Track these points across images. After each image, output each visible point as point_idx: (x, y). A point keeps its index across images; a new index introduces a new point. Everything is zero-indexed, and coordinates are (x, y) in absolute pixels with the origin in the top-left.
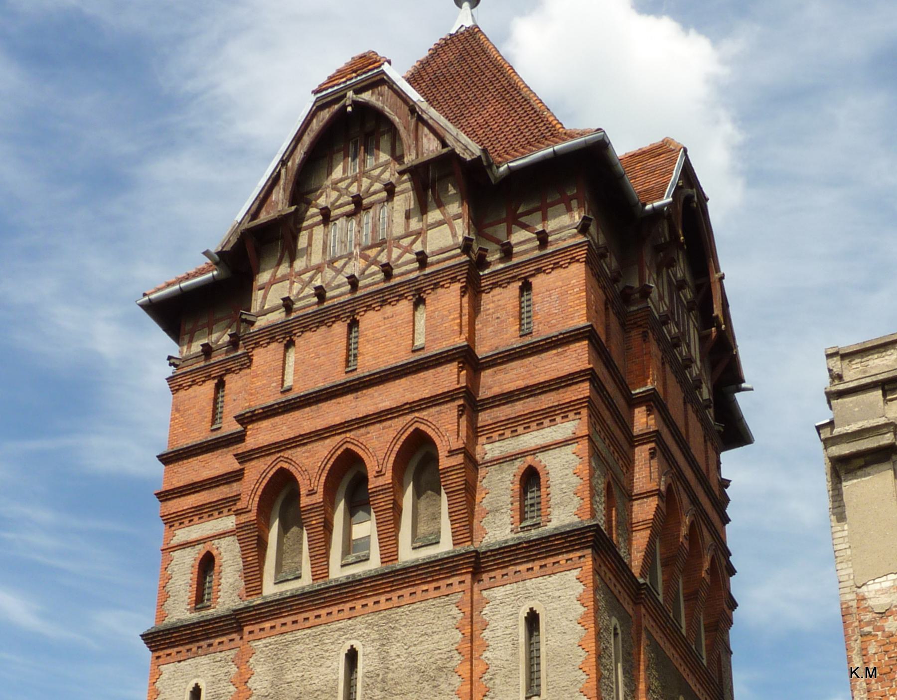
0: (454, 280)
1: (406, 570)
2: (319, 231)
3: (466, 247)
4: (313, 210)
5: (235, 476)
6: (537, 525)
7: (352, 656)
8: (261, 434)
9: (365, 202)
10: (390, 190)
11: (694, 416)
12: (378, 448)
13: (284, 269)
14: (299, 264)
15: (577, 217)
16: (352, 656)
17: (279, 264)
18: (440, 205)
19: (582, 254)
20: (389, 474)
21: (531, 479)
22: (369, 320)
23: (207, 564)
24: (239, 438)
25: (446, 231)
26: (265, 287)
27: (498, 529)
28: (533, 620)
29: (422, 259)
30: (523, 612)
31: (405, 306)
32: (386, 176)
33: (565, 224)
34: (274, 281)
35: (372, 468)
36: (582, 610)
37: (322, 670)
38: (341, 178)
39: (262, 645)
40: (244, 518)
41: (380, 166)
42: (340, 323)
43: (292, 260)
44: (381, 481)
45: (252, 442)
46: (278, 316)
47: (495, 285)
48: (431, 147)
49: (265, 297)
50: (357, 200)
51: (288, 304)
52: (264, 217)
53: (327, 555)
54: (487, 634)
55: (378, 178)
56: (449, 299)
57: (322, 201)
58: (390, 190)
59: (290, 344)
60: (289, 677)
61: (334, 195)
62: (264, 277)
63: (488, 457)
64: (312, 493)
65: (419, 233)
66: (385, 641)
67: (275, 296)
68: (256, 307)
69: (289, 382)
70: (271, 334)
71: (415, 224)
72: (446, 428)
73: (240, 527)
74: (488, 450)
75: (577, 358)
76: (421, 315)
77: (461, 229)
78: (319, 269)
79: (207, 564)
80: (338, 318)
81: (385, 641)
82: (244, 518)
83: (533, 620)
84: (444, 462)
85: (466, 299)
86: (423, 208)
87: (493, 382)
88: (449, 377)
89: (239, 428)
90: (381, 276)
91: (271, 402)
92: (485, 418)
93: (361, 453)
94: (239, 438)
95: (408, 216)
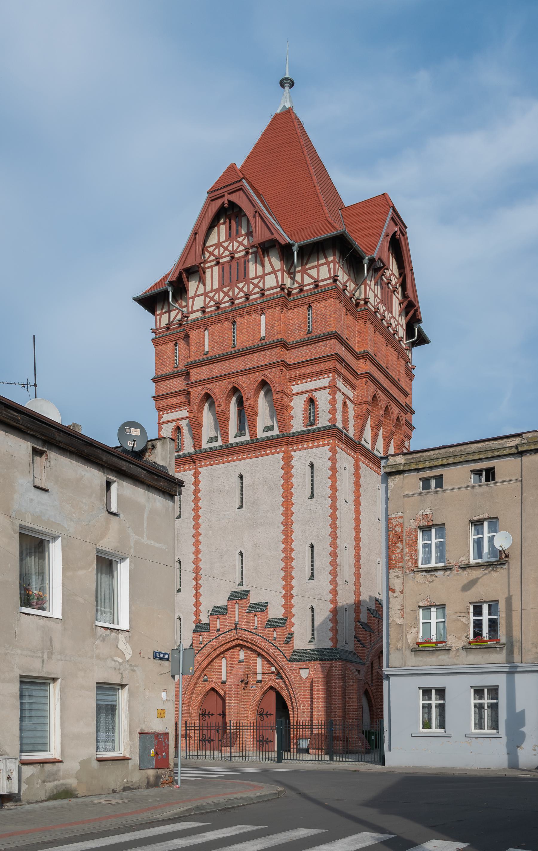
11: (382, 441)
42: (228, 322)
46: (199, 314)
93: (240, 388)
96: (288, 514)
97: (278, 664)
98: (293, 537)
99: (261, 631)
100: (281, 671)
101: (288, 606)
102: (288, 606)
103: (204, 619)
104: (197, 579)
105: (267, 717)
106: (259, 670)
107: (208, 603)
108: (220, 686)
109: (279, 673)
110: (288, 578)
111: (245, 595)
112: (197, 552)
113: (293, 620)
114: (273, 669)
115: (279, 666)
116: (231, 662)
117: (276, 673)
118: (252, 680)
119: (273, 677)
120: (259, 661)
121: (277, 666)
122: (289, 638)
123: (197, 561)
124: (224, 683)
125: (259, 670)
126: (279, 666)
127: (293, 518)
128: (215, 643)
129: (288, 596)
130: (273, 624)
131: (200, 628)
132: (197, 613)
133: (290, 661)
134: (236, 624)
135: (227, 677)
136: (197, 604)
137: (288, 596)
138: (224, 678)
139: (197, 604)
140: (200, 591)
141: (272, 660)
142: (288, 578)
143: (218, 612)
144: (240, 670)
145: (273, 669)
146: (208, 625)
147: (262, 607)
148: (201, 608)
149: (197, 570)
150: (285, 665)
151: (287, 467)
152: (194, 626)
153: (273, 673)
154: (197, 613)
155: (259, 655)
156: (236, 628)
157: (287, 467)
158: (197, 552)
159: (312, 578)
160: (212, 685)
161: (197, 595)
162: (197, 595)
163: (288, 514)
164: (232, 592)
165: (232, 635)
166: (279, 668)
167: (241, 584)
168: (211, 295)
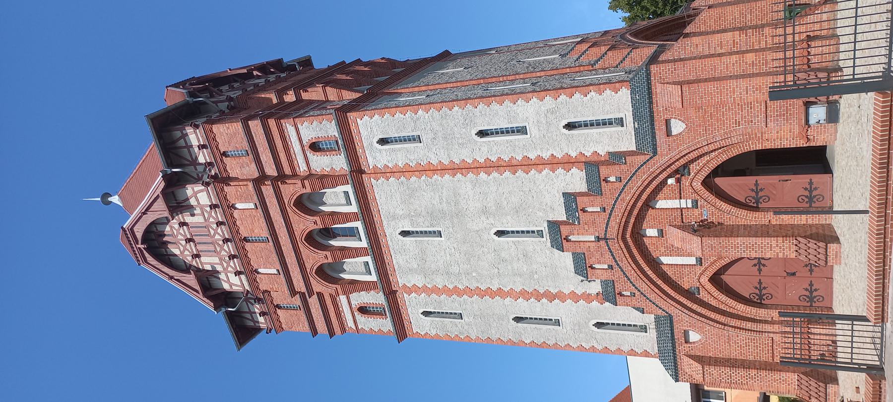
0: (222, 190)
1: (360, 207)
2: (203, 259)
3: (207, 184)
4: (194, 263)
5: (320, 296)
6: (337, 142)
7: (405, 234)
8: (300, 285)
9: (189, 237)
10: (183, 224)
12: (304, 224)
13: (222, 276)
14: (219, 268)
15: (189, 130)
16: (405, 234)
17: (219, 278)
18: (188, 199)
19: (207, 126)
20: (315, 218)
21: (315, 147)
22: (244, 233)
23: (363, 310)
24: (302, 295)
25: (199, 195)
26: (231, 285)
27: (338, 163)
28: (383, 141)
29: (213, 207)
30: (379, 146)
31: (236, 214)
32: (177, 226)
33: (194, 137)
34: (228, 281)
35: (312, 227)
36: (376, 116)
37: (411, 249)
38: (179, 250)
39: (401, 279)
40: (340, 291)
41: (172, 229)
43: (218, 272)
44: (319, 222)
45: (304, 290)
46: (243, 277)
47: (225, 170)
48: (160, 205)
49: (236, 285)
50: (189, 240)
51: (238, 273)
52: (198, 288)
53: (356, 249)
54: (390, 165)
55: (178, 231)
56: (230, 190)
57: (190, 258)
58: (183, 224)
59: (256, 271)
60: (416, 266)
61: (186, 253)
62: (226, 286)
63: (306, 169)
64: (326, 257)
65: (202, 209)
66: (394, 217)
67: (235, 280)
68: (240, 289)
69: (274, 271)
70: (253, 282)
71: (197, 211)
72: (291, 190)
73: (345, 293)
74: (302, 168)
75: (255, 126)
76: (238, 206)
77: (199, 187)
78: (221, 259)
79: (363, 310)
80: (243, 248)
81: (394, 217)
82: (340, 291)
83: (383, 141)
84: (308, 190)
85: (232, 184)
86: (191, 207)
87: (271, 170)
88: (268, 190)
89: (298, 296)
90: (223, 227)
91: (284, 279)
92: (288, 171)
94: (302, 295)
95: (193, 215)
96: (442, 169)
97: (661, 173)
98: (470, 161)
99: (609, 202)
100: (674, 167)
101: (567, 163)
102: (567, 163)
103: (595, 287)
104: (538, 296)
105: (761, 190)
106: (674, 204)
107: (572, 283)
108: (706, 269)
109: (677, 171)
110: (527, 165)
111: (554, 226)
112: (500, 293)
113: (588, 154)
114: (671, 181)
115: (664, 170)
116: (663, 250)
117: (678, 176)
118: (693, 217)
119: (686, 182)
120: (661, 204)
121: (664, 175)
122: (617, 158)
123: (511, 294)
124: (700, 261)
125: (674, 204)
126: (664, 170)
127: (446, 162)
128: (632, 273)
129: (553, 163)
130: (596, 184)
131: (610, 295)
132: (587, 298)
133: (655, 153)
134: (598, 239)
135: (690, 255)
136: (575, 297)
137: (553, 163)
138: (692, 261)
139: (575, 297)
140: (554, 291)
141: (655, 184)
142: (527, 165)
143: (583, 267)
144: (675, 236)
145: (671, 181)
146: (605, 284)
147: (570, 199)
148: (579, 292)
149: (525, 295)
150: (662, 160)
151: (386, 173)
152: (607, 304)
153: (678, 181)
154: (587, 298)
155: (649, 204)
156: (606, 239)
157: (386, 173)
158: (500, 293)
159: (522, 131)
160: (705, 280)
161: (560, 296)
162: (560, 296)
163: (442, 169)
164: (552, 246)
165: (617, 247)
166: (669, 171)
167: (540, 234)
168: (225, 265)
